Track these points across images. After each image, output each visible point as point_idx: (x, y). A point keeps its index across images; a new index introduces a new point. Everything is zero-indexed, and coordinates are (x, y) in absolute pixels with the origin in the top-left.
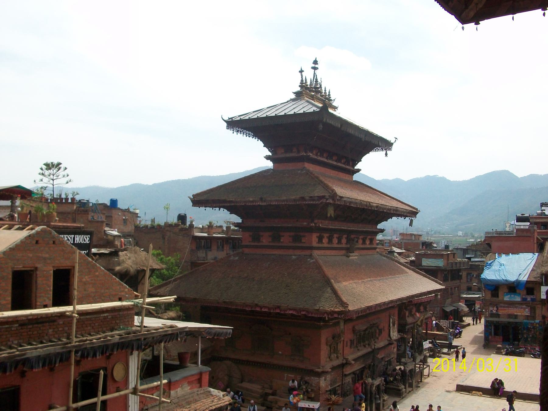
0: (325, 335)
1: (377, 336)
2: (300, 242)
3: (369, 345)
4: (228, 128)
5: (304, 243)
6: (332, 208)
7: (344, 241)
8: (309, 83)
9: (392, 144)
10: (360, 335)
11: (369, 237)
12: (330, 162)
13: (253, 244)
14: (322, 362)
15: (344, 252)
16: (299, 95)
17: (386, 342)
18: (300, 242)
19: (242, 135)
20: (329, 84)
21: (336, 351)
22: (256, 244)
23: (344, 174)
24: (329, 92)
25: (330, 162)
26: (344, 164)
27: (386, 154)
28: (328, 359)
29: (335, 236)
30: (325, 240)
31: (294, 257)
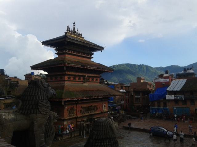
1: (96, 109)
3: (91, 112)
4: (42, 44)
7: (82, 79)
10: (86, 109)
12: (78, 54)
14: (65, 116)
15: (82, 83)
16: (66, 33)
17: (100, 112)
19: (48, 47)
20: (80, 29)
21: (73, 113)
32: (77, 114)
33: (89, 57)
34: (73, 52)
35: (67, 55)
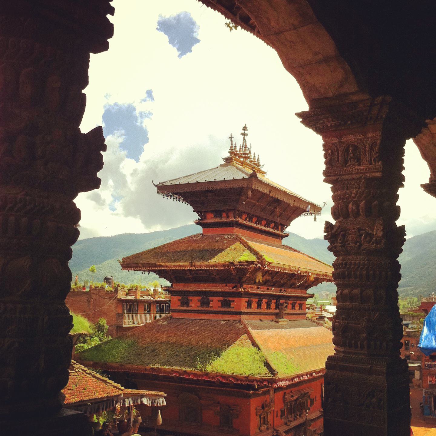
0: (254, 403)
1: (309, 406)
2: (230, 307)
5: (233, 307)
6: (261, 274)
7: (273, 305)
8: (238, 149)
9: (321, 209)
10: (291, 406)
11: (299, 302)
13: (182, 308)
16: (228, 161)
18: (229, 306)
19: (172, 199)
22: (185, 308)
23: (273, 239)
24: (258, 158)
25: (259, 227)
26: (273, 228)
27: (315, 219)
28: (258, 431)
29: (264, 300)
30: (254, 305)
31: (222, 322)
32: (275, 424)
33: (281, 233)
34: (248, 219)
35: (237, 231)
